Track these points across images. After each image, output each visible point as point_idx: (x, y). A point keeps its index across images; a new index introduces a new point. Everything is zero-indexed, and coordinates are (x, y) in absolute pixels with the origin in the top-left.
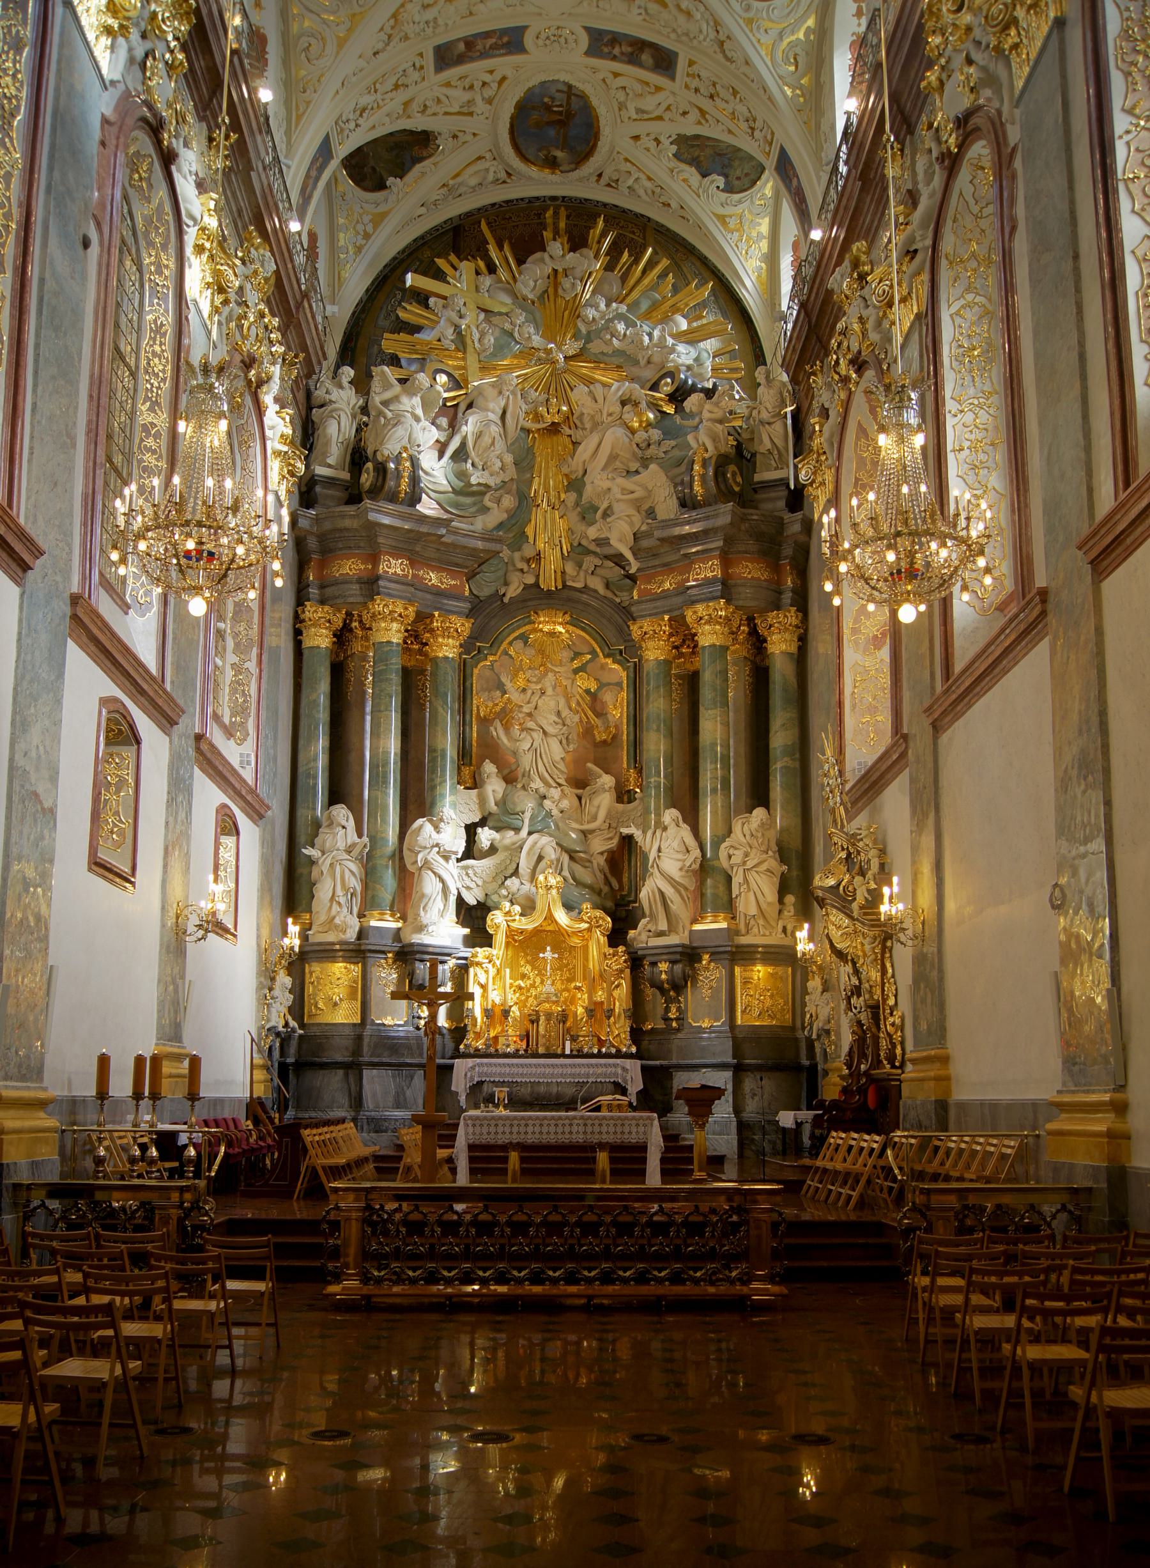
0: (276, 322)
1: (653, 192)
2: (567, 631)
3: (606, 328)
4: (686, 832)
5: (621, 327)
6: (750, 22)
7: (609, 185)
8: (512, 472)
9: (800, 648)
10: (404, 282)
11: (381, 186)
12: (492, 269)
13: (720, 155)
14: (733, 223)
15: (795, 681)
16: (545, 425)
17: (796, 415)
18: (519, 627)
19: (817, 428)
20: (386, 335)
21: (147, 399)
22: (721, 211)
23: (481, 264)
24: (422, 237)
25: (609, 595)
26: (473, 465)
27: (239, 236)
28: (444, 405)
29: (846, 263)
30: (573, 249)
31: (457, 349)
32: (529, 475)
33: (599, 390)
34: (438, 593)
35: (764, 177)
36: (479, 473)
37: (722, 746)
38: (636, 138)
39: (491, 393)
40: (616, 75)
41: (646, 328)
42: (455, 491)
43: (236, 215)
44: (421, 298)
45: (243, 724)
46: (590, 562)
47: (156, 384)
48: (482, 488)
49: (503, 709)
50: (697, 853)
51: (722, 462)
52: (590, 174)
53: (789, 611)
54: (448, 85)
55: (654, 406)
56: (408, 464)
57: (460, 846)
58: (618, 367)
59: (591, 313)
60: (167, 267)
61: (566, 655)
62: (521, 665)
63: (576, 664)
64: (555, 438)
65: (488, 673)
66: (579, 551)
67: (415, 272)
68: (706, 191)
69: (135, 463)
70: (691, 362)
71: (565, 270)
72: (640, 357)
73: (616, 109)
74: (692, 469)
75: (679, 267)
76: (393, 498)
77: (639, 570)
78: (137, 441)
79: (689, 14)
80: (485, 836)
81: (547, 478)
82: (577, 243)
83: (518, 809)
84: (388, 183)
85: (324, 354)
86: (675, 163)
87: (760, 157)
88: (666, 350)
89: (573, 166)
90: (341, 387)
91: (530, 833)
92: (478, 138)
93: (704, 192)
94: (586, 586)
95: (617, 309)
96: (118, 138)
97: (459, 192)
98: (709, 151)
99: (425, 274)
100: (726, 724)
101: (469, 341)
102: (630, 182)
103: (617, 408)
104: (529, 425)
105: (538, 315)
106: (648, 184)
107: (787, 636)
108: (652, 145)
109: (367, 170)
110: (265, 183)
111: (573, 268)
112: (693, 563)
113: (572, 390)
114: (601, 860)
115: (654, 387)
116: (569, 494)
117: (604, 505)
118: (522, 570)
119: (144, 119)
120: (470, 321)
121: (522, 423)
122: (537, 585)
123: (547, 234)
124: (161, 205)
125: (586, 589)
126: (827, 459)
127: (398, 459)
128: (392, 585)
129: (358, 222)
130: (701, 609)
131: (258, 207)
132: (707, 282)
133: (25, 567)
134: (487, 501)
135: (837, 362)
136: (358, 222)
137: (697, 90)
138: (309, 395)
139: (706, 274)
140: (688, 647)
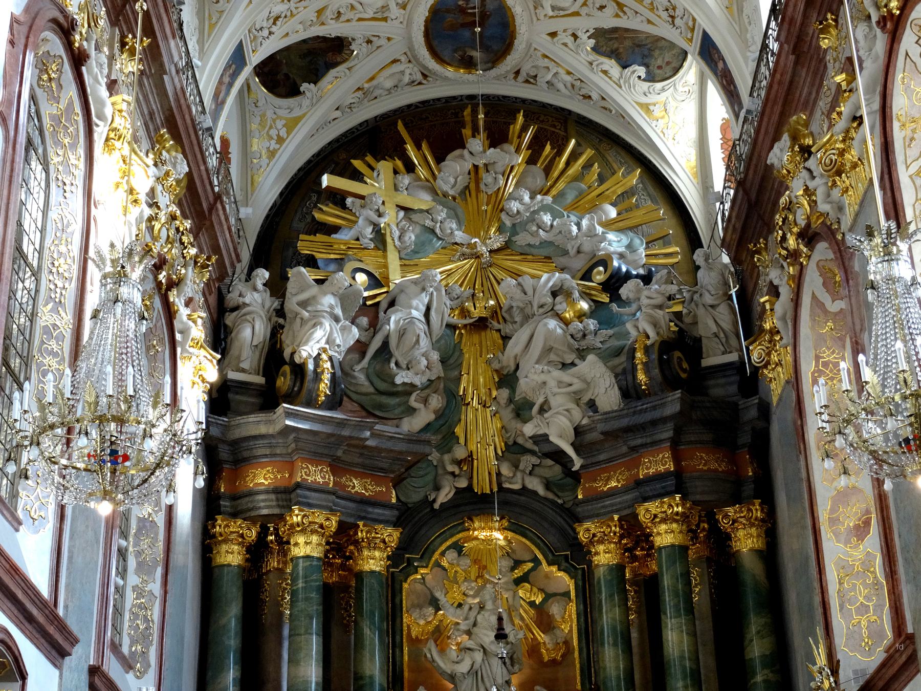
0: (188, 224)
1: (573, 86)
2: (506, 538)
5: (547, 218)
7: (527, 81)
8: (438, 370)
9: (768, 544)
10: (321, 184)
11: (294, 92)
12: (410, 168)
13: (639, 46)
14: (658, 111)
15: (765, 581)
16: (472, 321)
17: (740, 295)
18: (452, 536)
19: (768, 306)
20: (302, 237)
22: (644, 100)
23: (399, 163)
24: (336, 140)
25: (550, 496)
26: (397, 364)
27: (150, 138)
28: (364, 304)
29: (786, 137)
31: (377, 248)
32: (456, 373)
33: (527, 282)
34: (363, 501)
35: (686, 64)
36: (404, 373)
37: (690, 659)
38: (553, 35)
39: (414, 289)
41: (573, 218)
43: (148, 118)
44: (338, 198)
46: (527, 461)
47: (60, 284)
48: (408, 388)
51: (666, 346)
52: (507, 72)
53: (754, 505)
55: (585, 295)
56: (328, 365)
58: (546, 258)
59: (514, 206)
60: (76, 166)
61: (506, 563)
62: (455, 577)
63: (518, 573)
64: (483, 334)
65: (419, 587)
67: (331, 173)
68: (627, 81)
69: (34, 367)
71: (486, 165)
72: (569, 247)
73: (532, 8)
74: (634, 357)
75: (603, 157)
77: (582, 467)
78: (37, 343)
82: (497, 138)
84: (302, 89)
85: (238, 256)
86: (593, 57)
87: (684, 45)
88: (595, 239)
89: (490, 65)
90: (255, 289)
92: (392, 42)
93: (625, 82)
94: (524, 488)
95: (542, 201)
96: (28, 37)
97: (375, 94)
98: (628, 43)
99: (341, 174)
100: (693, 634)
101: (389, 240)
102: (549, 77)
103: (549, 300)
104: (456, 320)
105: (460, 211)
106: (568, 78)
107: (753, 531)
108: (569, 40)
109: (280, 77)
110: (178, 86)
111: (494, 163)
112: (641, 456)
113: (499, 283)
116: (501, 391)
117: (541, 400)
118: (453, 474)
119: (54, 21)
120: (390, 219)
121: (447, 319)
122: (470, 488)
123: (467, 132)
124: (71, 103)
125: (524, 490)
126: (781, 338)
127: (317, 359)
128: (313, 494)
129: (271, 127)
130: (653, 507)
131: (171, 109)
132: (633, 170)
134: (413, 401)
135: (784, 238)
136: (271, 127)
138: (221, 298)
139: (631, 162)
140: (642, 549)
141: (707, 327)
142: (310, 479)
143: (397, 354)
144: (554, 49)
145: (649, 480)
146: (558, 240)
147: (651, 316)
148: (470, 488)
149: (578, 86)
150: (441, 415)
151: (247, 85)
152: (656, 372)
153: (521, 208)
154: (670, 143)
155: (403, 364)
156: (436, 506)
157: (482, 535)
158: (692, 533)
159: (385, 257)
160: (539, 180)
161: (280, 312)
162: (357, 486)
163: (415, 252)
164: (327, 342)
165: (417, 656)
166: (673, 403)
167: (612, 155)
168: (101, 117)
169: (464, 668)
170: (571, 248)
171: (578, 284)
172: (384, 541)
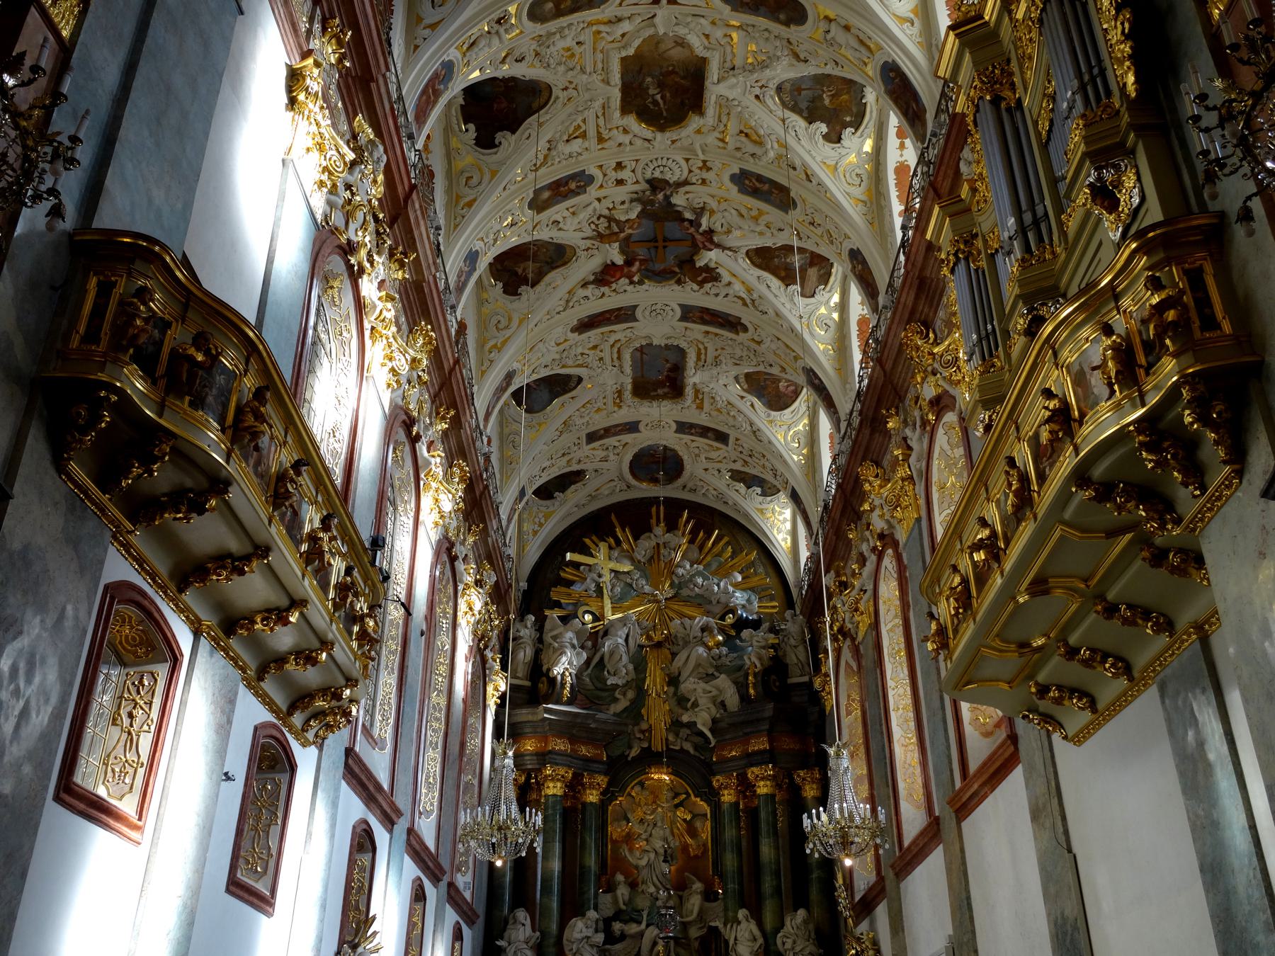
3: (690, 580)
4: (753, 926)
5: (700, 580)
6: (771, 422)
8: (632, 675)
21: (436, 689)
22: (760, 507)
23: (612, 540)
25: (697, 754)
30: (668, 531)
31: (597, 596)
34: (586, 760)
38: (706, 470)
39: (621, 625)
40: (693, 441)
42: (597, 689)
44: (576, 565)
45: (466, 862)
46: (684, 732)
49: (628, 834)
50: (761, 941)
54: (594, 449)
55: (722, 630)
57: (600, 938)
59: (680, 571)
61: (670, 795)
63: (677, 801)
65: (617, 808)
66: (676, 725)
74: (747, 679)
79: (734, 416)
80: (617, 926)
81: (655, 675)
82: (672, 526)
83: (640, 908)
90: (526, 627)
91: (648, 926)
94: (682, 748)
100: (777, 848)
101: (605, 591)
103: (700, 634)
104: (643, 640)
106: (715, 493)
107: (815, 786)
108: (716, 473)
114: (696, 944)
115: (723, 618)
117: (693, 700)
120: (607, 577)
122: (650, 747)
123: (654, 521)
130: (756, 770)
133: (393, 823)
137: (741, 452)
141: (791, 659)
142: (557, 748)
143: (608, 666)
144: (707, 477)
145: (755, 753)
146: (706, 594)
147: (758, 653)
149: (720, 497)
150: (633, 702)
151: (506, 404)
152: (760, 689)
153: (685, 572)
154: (775, 532)
155: (612, 672)
156: (629, 759)
157: (656, 777)
158: (778, 786)
159: (602, 602)
160: (695, 554)
161: (540, 640)
162: (584, 751)
165: (615, 851)
166: (769, 709)
168: (461, 582)
169: (643, 862)
171: (717, 624)
172: (598, 784)
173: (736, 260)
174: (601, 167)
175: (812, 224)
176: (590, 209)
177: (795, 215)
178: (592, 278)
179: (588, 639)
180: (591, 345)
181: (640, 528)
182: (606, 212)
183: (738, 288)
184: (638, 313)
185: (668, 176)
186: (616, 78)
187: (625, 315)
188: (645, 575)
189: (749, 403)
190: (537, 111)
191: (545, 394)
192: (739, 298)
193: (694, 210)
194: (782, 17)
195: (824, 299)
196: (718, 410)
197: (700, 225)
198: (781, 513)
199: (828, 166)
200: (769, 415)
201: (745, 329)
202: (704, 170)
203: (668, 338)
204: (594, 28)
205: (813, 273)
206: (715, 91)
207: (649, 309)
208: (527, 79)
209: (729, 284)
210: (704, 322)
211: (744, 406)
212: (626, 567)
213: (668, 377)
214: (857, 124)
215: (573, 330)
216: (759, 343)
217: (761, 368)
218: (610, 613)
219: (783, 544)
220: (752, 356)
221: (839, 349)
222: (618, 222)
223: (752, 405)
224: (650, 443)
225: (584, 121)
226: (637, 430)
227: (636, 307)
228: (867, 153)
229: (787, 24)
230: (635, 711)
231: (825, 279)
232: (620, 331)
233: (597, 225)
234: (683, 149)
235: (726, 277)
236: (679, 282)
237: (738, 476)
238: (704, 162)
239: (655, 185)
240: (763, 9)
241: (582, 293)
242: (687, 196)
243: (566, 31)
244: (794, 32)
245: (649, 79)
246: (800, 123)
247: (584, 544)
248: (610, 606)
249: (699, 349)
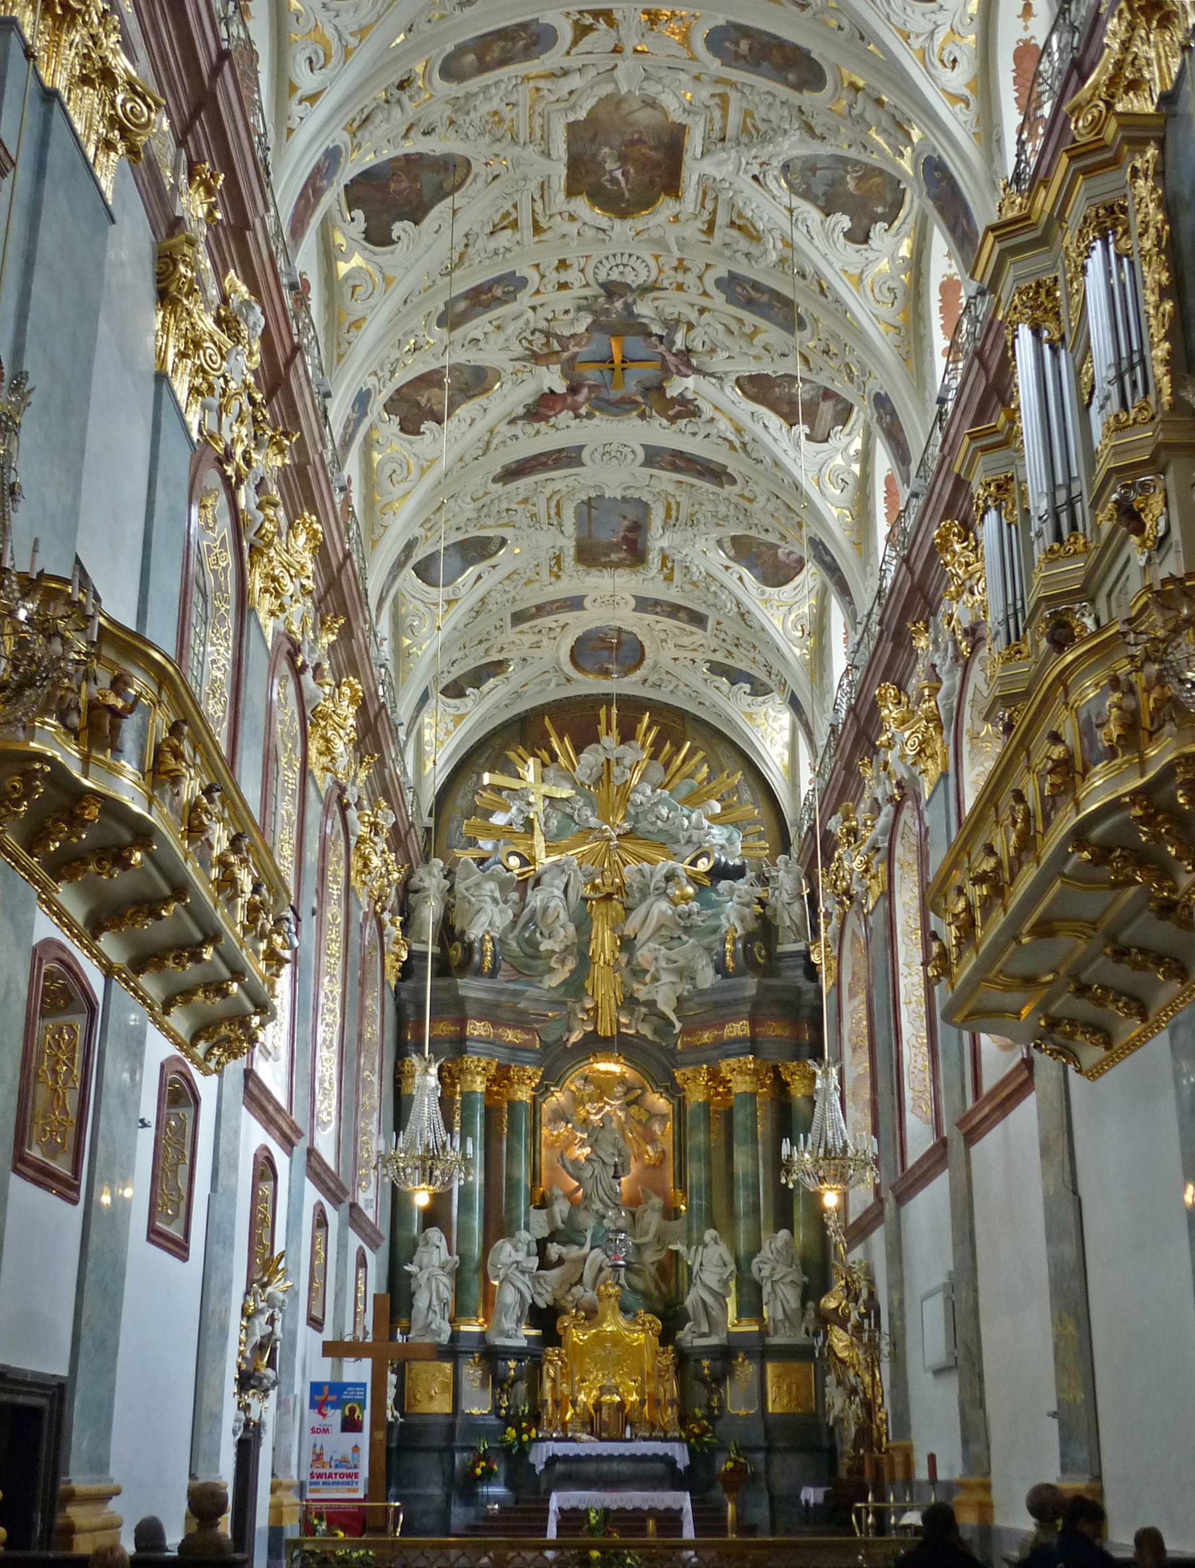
5: (664, 811)
6: (766, 602)
11: (461, 694)
22: (748, 710)
23: (545, 755)
30: (622, 742)
41: (686, 812)
44: (498, 789)
51: (749, 938)
54: (522, 632)
55: (693, 879)
56: (489, 945)
59: (638, 798)
66: (629, 1002)
70: (723, 842)
76: (478, 972)
82: (627, 735)
90: (430, 873)
101: (536, 824)
104: (587, 891)
106: (686, 690)
115: (693, 863)
122: (595, 1031)
123: (602, 728)
127: (482, 940)
144: (677, 669)
148: (595, 1031)
150: (572, 972)
154: (768, 745)
155: (546, 933)
160: (657, 773)
161: (451, 890)
163: (556, 835)
164: (490, 924)
167: (722, 750)
170: (683, 835)
173: (722, 388)
174: (537, 266)
175: (826, 352)
176: (521, 322)
177: (806, 339)
178: (521, 411)
179: (515, 890)
180: (520, 498)
181: (584, 738)
182: (543, 325)
183: (723, 425)
184: (585, 455)
185: (630, 278)
186: (560, 148)
187: (567, 458)
188: (590, 803)
189: (735, 576)
190: (451, 193)
191: (456, 562)
192: (725, 439)
193: (665, 323)
194: (791, 77)
195: (842, 445)
196: (694, 584)
197: (673, 343)
198: (775, 719)
199: (850, 276)
200: (763, 593)
201: (733, 481)
202: (680, 272)
203: (625, 489)
204: (532, 84)
205: (826, 409)
206: (694, 170)
207: (600, 450)
208: (438, 153)
209: (712, 420)
210: (676, 469)
211: (730, 580)
212: (565, 792)
213: (625, 538)
214: (891, 218)
215: (495, 480)
216: (751, 501)
217: (753, 533)
218: (543, 854)
219: (778, 761)
220: (741, 517)
221: (859, 515)
222: (559, 338)
223: (741, 579)
224: (598, 624)
225: (515, 206)
226: (582, 608)
227: (582, 447)
228: (903, 258)
229: (798, 87)
230: (576, 986)
231: (844, 414)
232: (559, 479)
233: (530, 342)
234: (651, 241)
235: (708, 411)
236: (642, 416)
237: (717, 669)
238: (681, 260)
239: (612, 290)
240: (765, 65)
241: (504, 430)
242: (657, 303)
243: (493, 90)
244: (807, 98)
245: (606, 150)
246: (811, 213)
247: (507, 759)
248: (543, 844)
249: (669, 505)
